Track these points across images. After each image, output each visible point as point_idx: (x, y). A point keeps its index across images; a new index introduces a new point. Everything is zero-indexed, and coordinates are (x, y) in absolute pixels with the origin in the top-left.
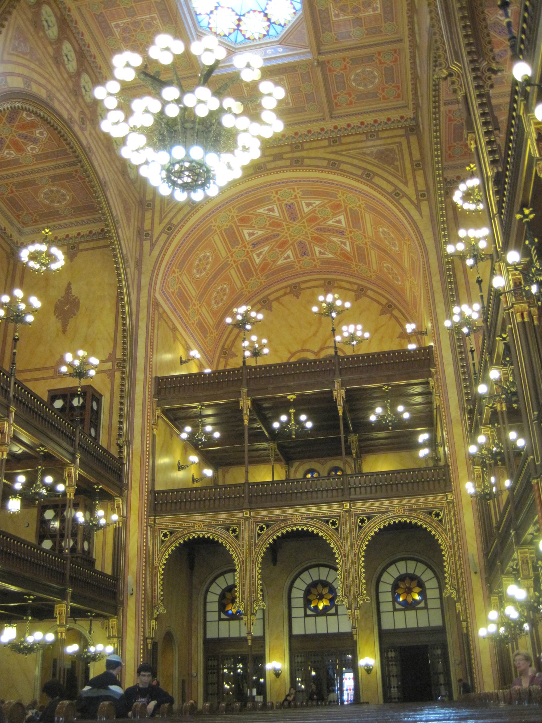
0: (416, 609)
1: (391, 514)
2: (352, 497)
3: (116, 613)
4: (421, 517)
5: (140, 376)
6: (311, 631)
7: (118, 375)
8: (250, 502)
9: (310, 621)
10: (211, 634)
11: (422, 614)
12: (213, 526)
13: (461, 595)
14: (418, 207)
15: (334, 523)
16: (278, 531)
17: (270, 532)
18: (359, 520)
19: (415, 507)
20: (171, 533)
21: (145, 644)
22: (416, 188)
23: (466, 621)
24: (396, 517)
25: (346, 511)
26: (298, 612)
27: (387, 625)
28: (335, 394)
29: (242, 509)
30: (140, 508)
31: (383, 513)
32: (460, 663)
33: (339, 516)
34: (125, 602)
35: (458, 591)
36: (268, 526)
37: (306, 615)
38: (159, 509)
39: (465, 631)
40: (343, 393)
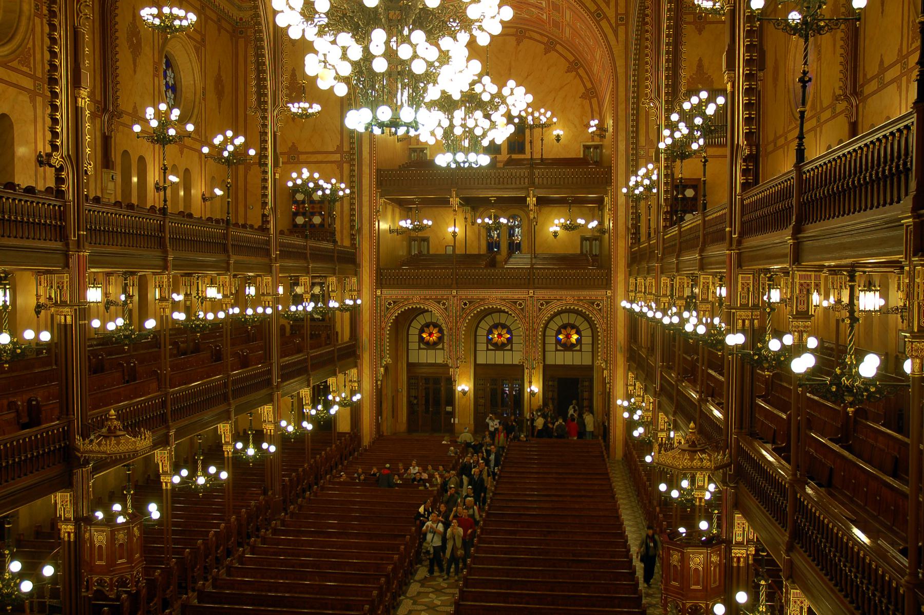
0: (573, 351)
1: (564, 302)
3: (356, 366)
4: (586, 306)
5: (366, 170)
6: (491, 361)
7: (346, 166)
8: (457, 283)
12: (428, 299)
14: (616, 32)
16: (478, 307)
20: (394, 302)
21: (377, 385)
22: (617, 10)
23: (609, 383)
24: (567, 304)
26: (482, 347)
27: (550, 361)
28: (528, 199)
29: (449, 287)
30: (371, 282)
31: (558, 300)
35: (606, 362)
36: (470, 303)
37: (488, 349)
38: (384, 282)
39: (608, 390)
40: (535, 199)
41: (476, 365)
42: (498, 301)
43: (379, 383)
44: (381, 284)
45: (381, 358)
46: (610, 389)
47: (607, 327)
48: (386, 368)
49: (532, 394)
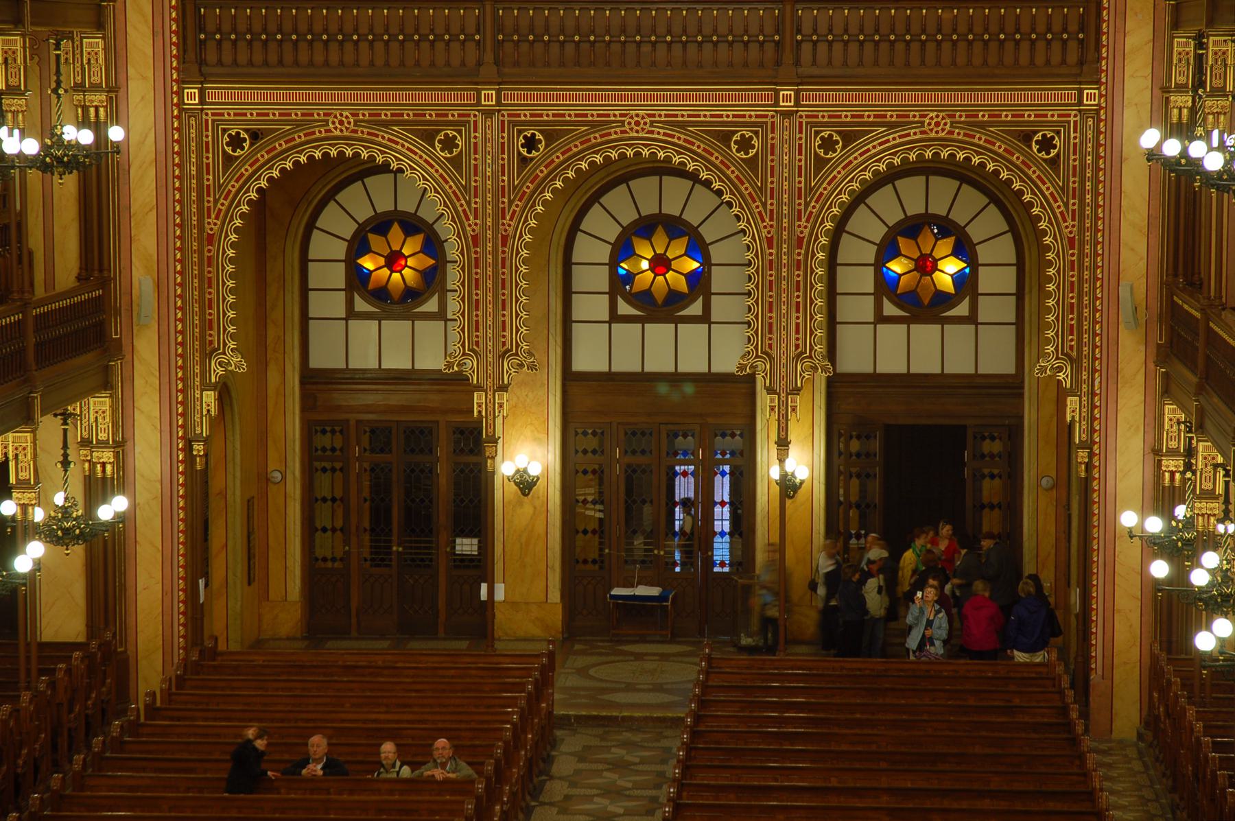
2: (805, 70)
4: (1000, 147)
8: (497, 62)
9: (627, 333)
10: (325, 356)
11: (959, 335)
12: (386, 124)
13: (1085, 376)
15: (745, 144)
16: (579, 156)
17: (558, 158)
18: (818, 142)
19: (983, 117)
20: (255, 136)
21: (190, 459)
23: (1088, 445)
24: (926, 142)
25: (787, 114)
26: (592, 307)
27: (854, 360)
29: (470, 76)
31: (891, 126)
32: (1056, 486)
33: (761, 125)
34: (125, 341)
35: (1076, 362)
36: (551, 137)
37: (614, 317)
38: (211, 57)
41: (569, 377)
42: (660, 133)
43: (198, 448)
44: (202, 62)
45: (208, 352)
46: (1089, 466)
47: (1082, 230)
48: (224, 391)
49: (788, 487)
